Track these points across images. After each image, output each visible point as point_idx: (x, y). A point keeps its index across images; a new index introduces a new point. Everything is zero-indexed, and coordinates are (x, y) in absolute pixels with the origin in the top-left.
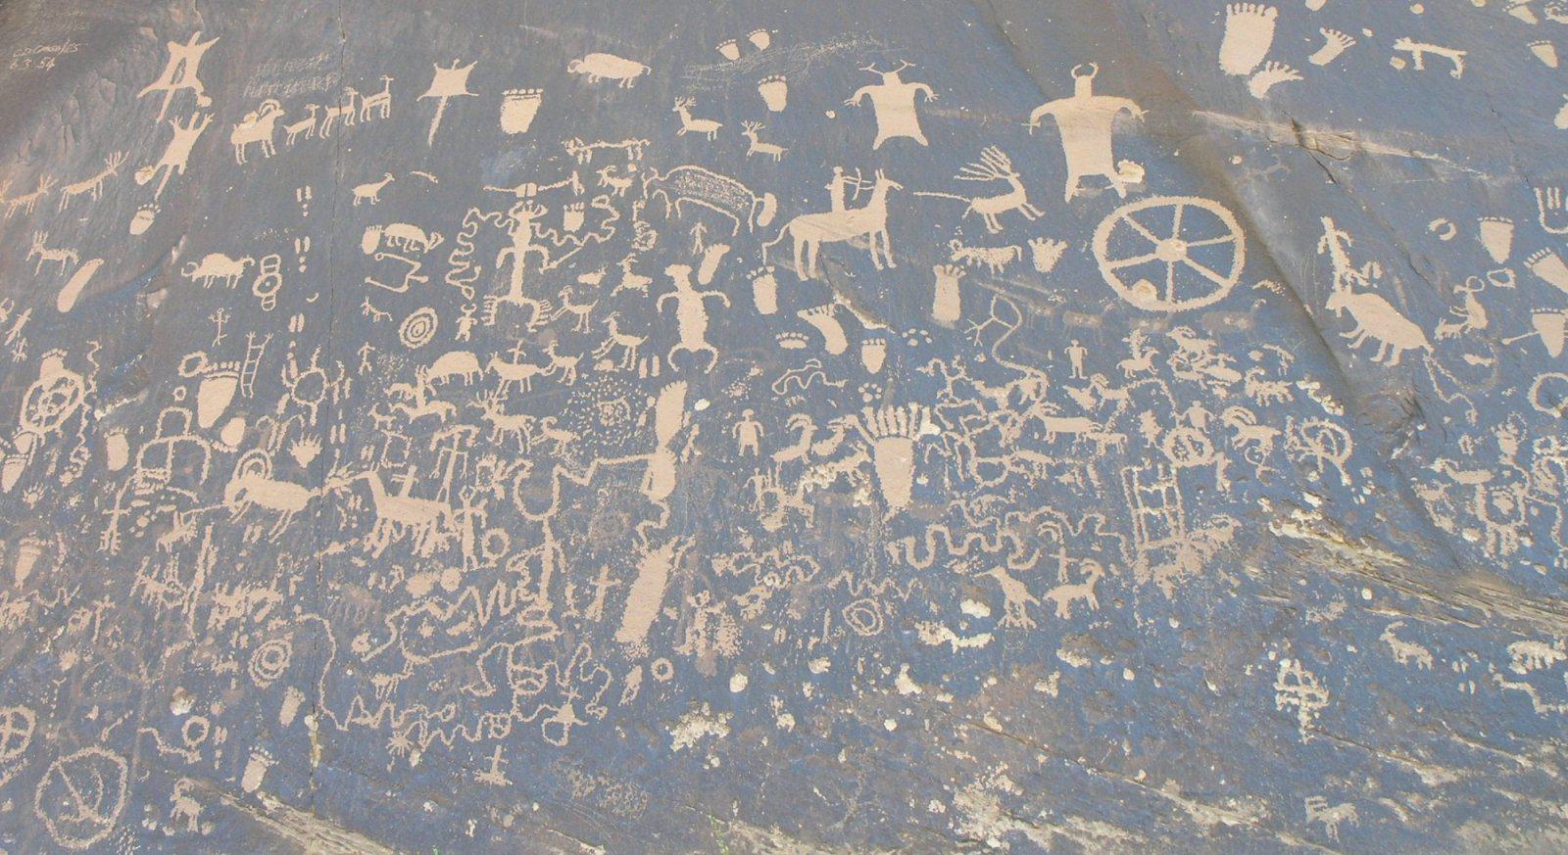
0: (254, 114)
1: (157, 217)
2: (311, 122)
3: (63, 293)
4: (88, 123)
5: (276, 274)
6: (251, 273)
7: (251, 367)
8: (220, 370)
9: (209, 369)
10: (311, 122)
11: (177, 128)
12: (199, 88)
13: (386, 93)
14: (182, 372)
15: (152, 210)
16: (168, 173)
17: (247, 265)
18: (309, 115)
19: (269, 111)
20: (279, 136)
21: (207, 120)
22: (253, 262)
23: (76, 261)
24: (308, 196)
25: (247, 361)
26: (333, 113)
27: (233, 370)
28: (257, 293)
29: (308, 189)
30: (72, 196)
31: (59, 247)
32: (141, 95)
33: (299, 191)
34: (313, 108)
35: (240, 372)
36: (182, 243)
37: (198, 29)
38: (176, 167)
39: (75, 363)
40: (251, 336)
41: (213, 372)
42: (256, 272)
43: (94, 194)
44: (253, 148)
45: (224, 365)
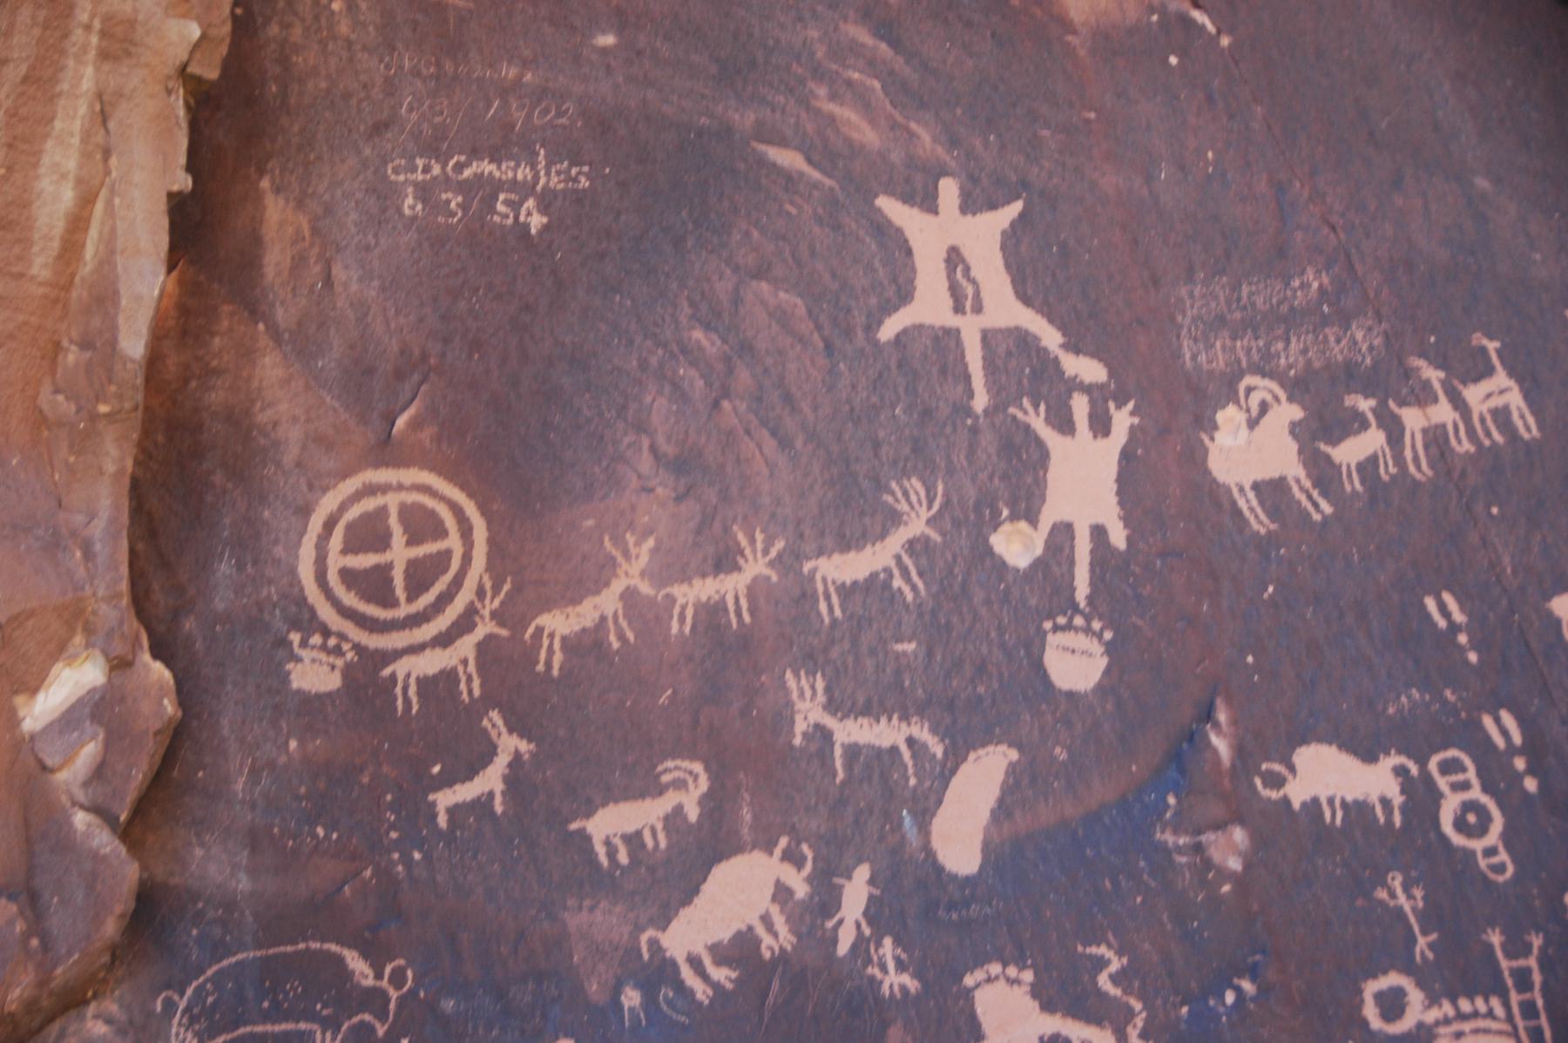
0: (1231, 410)
1: (1110, 648)
2: (1372, 441)
3: (939, 825)
4: (788, 398)
5: (1476, 793)
6: (1421, 796)
7: (1529, 1010)
8: (1461, 1017)
9: (1433, 1015)
10: (1372, 441)
11: (1038, 424)
12: (1051, 338)
13: (1501, 379)
14: (1371, 1012)
15: (1087, 630)
16: (1083, 548)
17: (1400, 771)
18: (1365, 425)
19: (1264, 408)
20: (1323, 474)
21: (1123, 420)
22: (1414, 769)
23: (938, 750)
24: (1459, 617)
25: (1515, 998)
26: (1413, 419)
27: (1490, 1014)
28: (1458, 840)
29: (1448, 598)
30: (847, 592)
31: (869, 710)
32: (889, 329)
33: (1430, 604)
34: (1365, 405)
35: (1510, 1018)
36: (1222, 716)
37: (944, 172)
38: (1099, 532)
39: (1065, 992)
40: (1495, 938)
41: (1447, 1021)
42: (1436, 797)
43: (897, 582)
44: (1272, 492)
45: (1465, 1006)
